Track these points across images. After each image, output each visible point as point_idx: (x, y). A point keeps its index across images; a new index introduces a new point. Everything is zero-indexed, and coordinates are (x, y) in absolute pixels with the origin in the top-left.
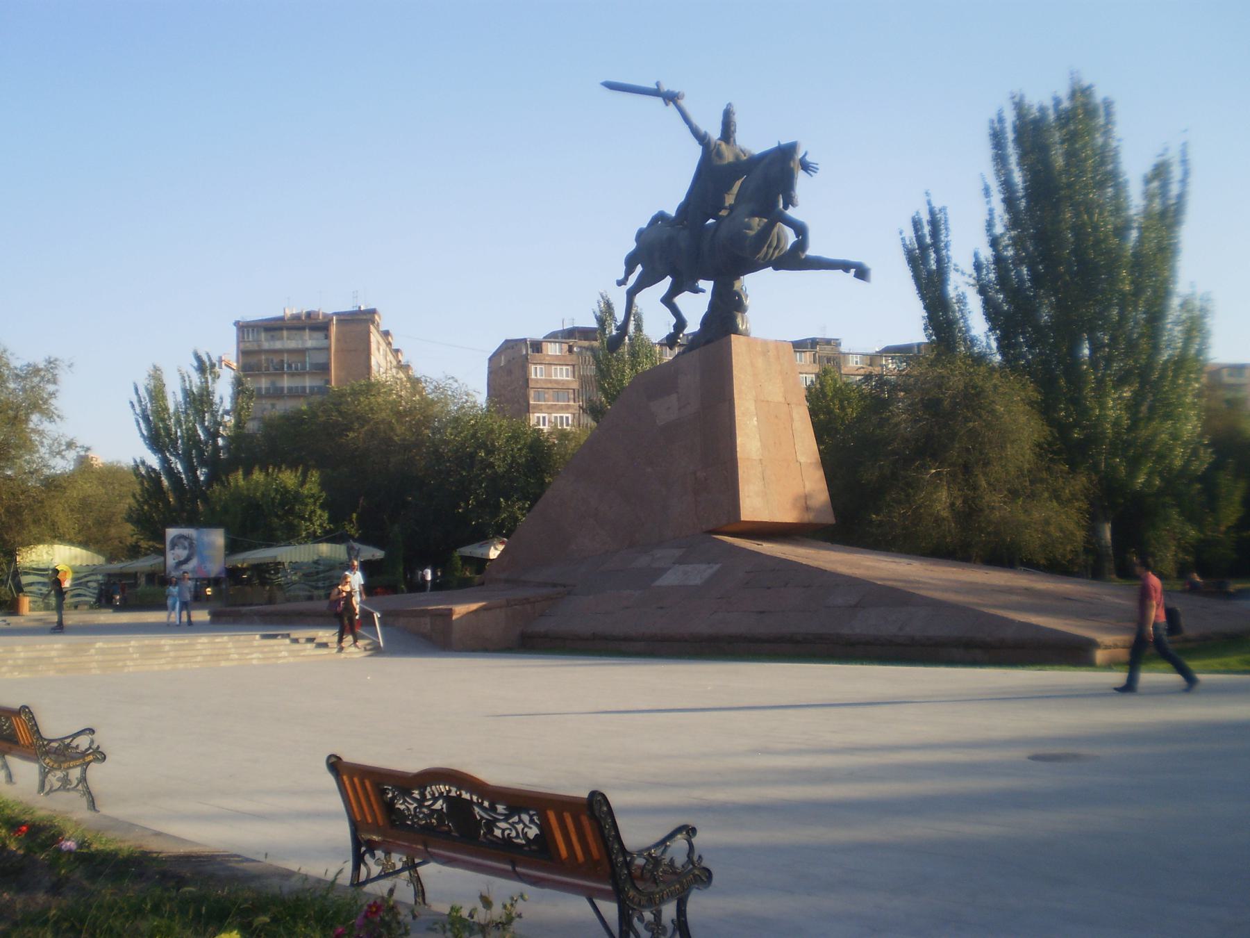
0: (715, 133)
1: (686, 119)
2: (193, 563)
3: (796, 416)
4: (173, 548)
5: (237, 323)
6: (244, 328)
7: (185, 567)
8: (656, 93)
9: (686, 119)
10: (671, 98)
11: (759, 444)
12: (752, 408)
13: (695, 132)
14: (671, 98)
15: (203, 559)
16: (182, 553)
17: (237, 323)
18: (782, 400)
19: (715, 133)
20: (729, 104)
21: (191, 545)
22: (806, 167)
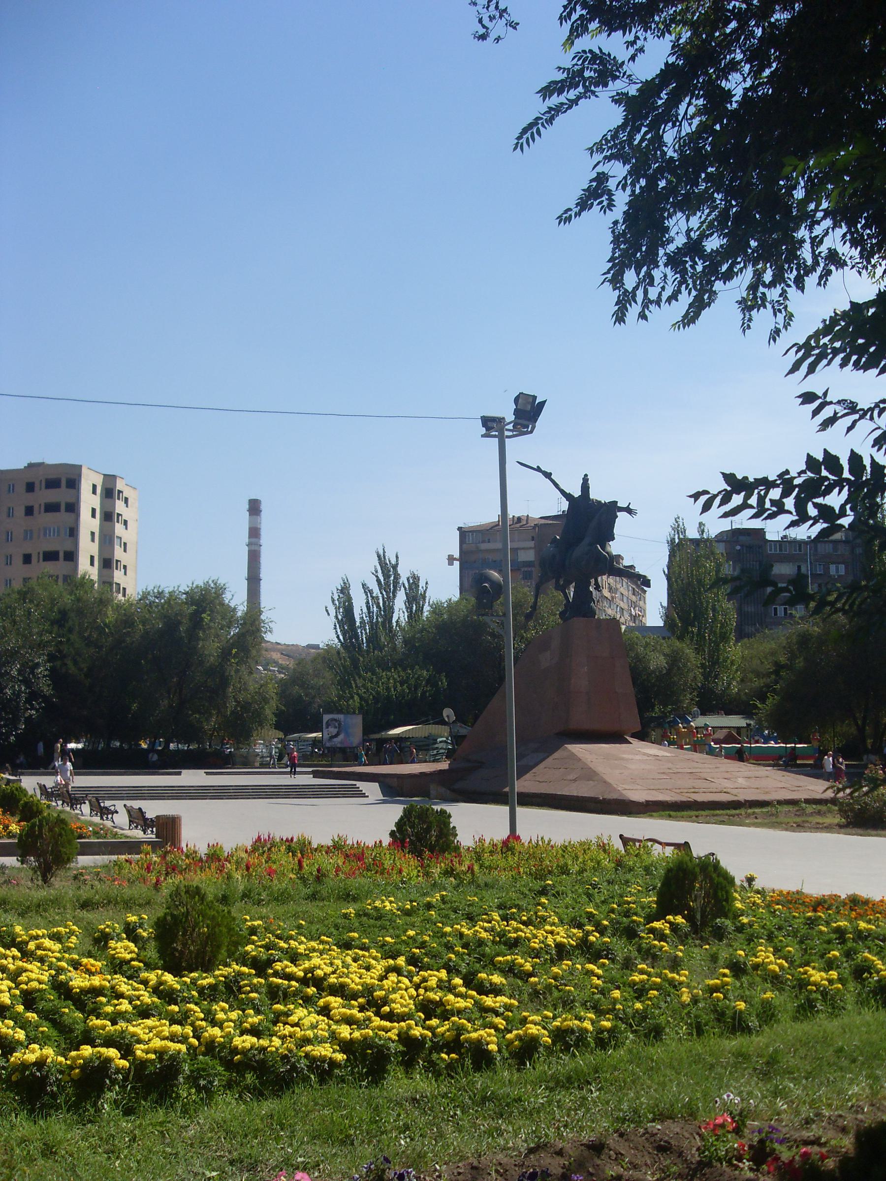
0: (577, 493)
1: (556, 485)
2: (341, 737)
4: (327, 727)
5: (460, 529)
6: (463, 533)
7: (335, 739)
8: (538, 469)
9: (556, 485)
10: (548, 475)
13: (563, 492)
14: (548, 475)
15: (348, 735)
16: (333, 731)
17: (460, 529)
19: (577, 493)
20: (586, 475)
21: (340, 724)
22: (628, 510)
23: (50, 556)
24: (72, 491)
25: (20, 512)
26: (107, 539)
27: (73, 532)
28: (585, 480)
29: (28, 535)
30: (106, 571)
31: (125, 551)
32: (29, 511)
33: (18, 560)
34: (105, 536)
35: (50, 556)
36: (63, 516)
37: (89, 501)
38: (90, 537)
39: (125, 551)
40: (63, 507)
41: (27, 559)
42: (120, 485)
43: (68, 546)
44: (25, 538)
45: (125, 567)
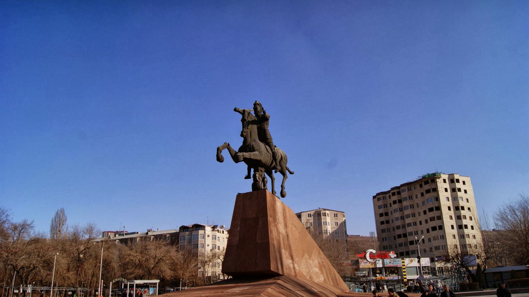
3: (260, 222)
11: (238, 238)
12: (239, 223)
18: (254, 216)
23: (431, 210)
24: (434, 184)
25: (419, 195)
26: (455, 199)
27: (437, 199)
28: (255, 104)
29: (423, 203)
30: (457, 212)
31: (468, 202)
32: (422, 194)
33: (422, 213)
34: (454, 198)
35: (431, 210)
36: (433, 194)
37: (442, 185)
38: (446, 199)
39: (468, 202)
40: (431, 190)
41: (425, 212)
42: (456, 177)
43: (437, 205)
44: (423, 205)
45: (469, 209)
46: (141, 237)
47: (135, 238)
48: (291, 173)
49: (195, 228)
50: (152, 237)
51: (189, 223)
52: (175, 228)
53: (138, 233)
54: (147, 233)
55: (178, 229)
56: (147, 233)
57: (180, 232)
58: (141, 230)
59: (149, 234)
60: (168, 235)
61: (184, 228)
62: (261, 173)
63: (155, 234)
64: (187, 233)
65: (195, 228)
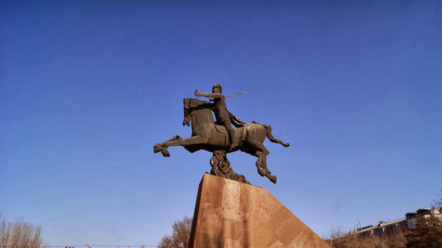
46: (374, 230)
47: (370, 231)
48: (285, 146)
49: (420, 214)
50: (383, 229)
51: (414, 210)
52: (402, 217)
53: (372, 226)
54: (379, 225)
55: (405, 217)
56: (379, 225)
57: (407, 219)
58: (375, 224)
59: (381, 225)
60: (397, 225)
61: (409, 216)
62: (218, 156)
63: (386, 224)
64: (414, 219)
65: (420, 214)
